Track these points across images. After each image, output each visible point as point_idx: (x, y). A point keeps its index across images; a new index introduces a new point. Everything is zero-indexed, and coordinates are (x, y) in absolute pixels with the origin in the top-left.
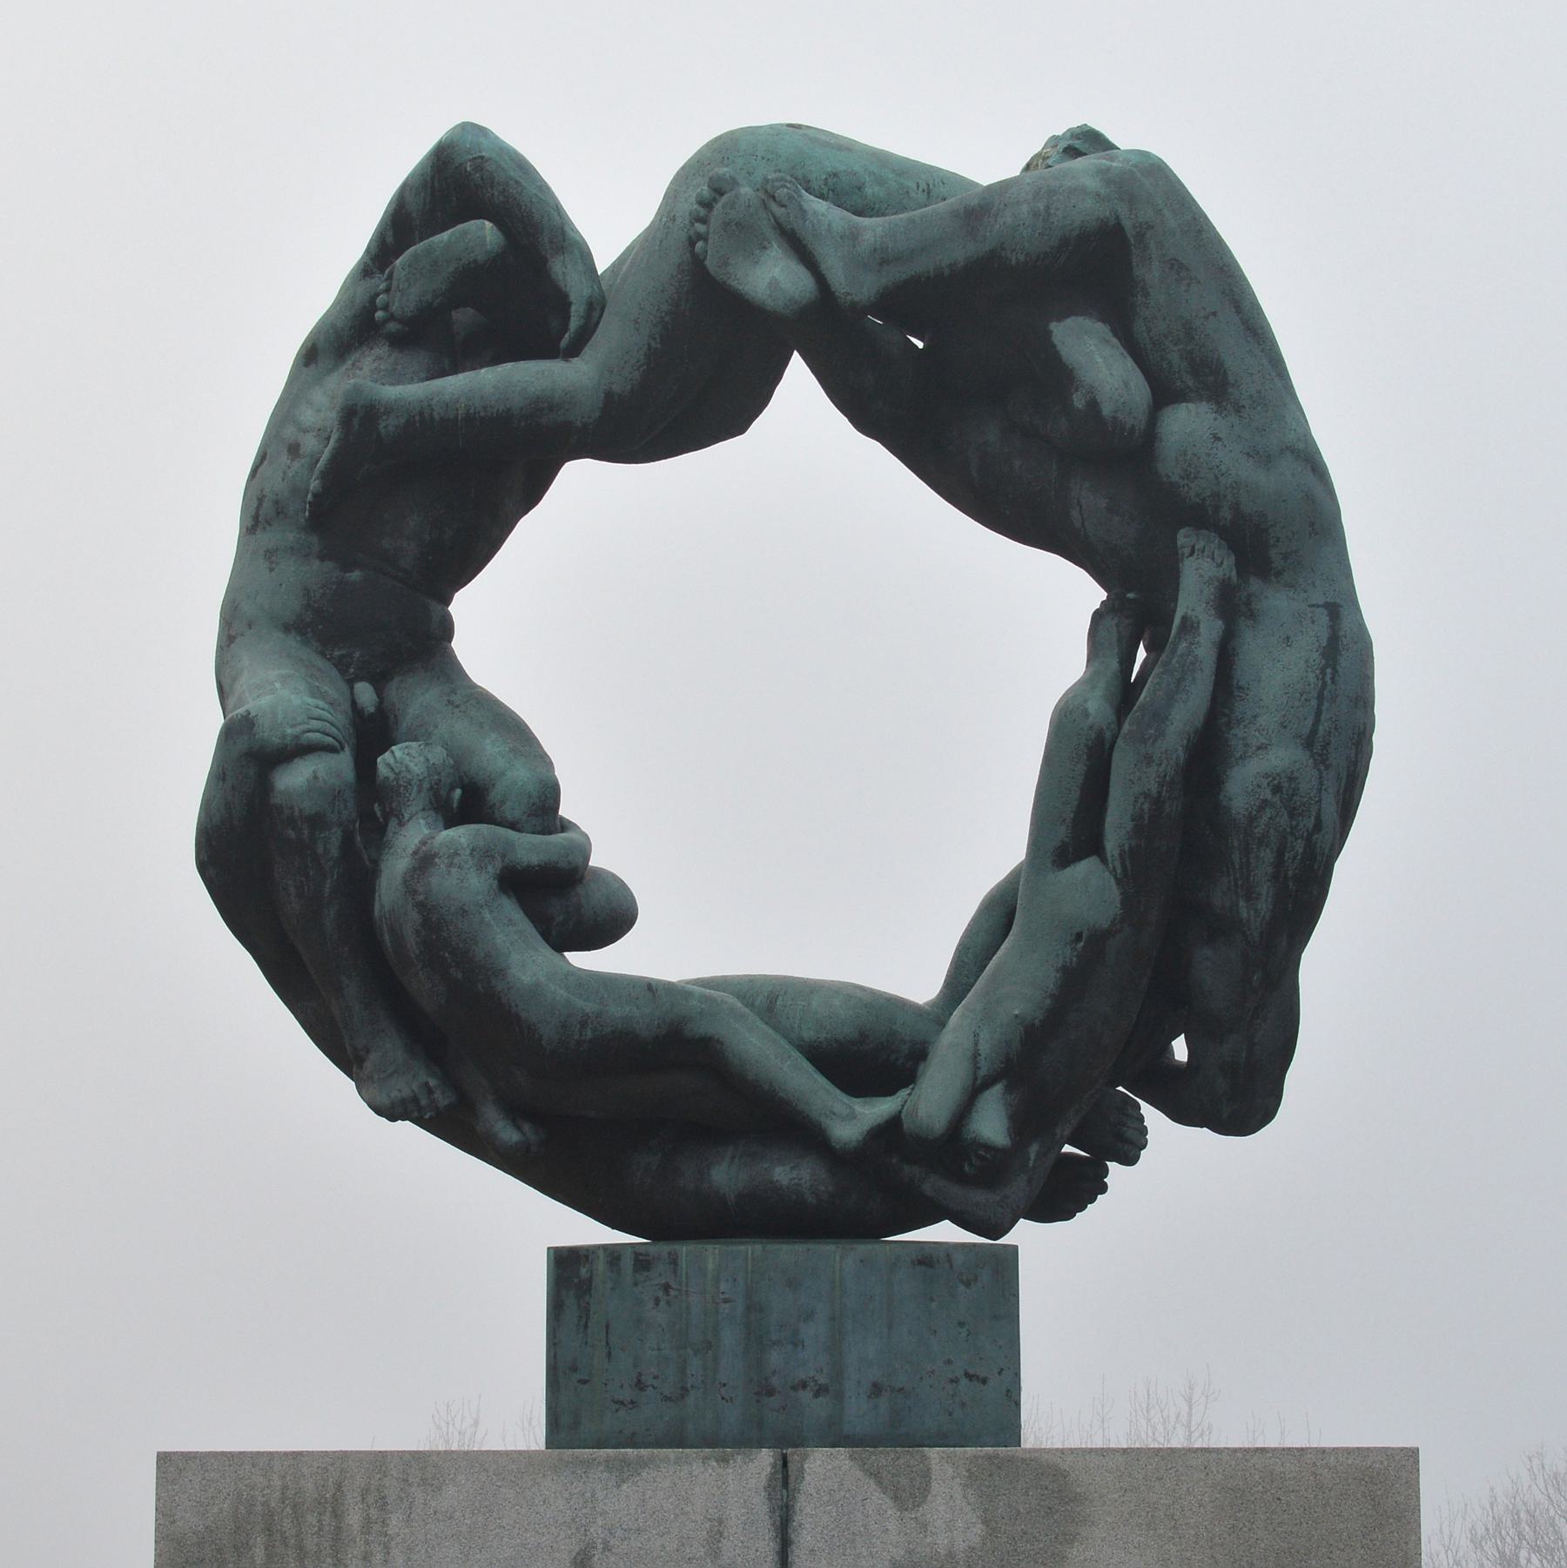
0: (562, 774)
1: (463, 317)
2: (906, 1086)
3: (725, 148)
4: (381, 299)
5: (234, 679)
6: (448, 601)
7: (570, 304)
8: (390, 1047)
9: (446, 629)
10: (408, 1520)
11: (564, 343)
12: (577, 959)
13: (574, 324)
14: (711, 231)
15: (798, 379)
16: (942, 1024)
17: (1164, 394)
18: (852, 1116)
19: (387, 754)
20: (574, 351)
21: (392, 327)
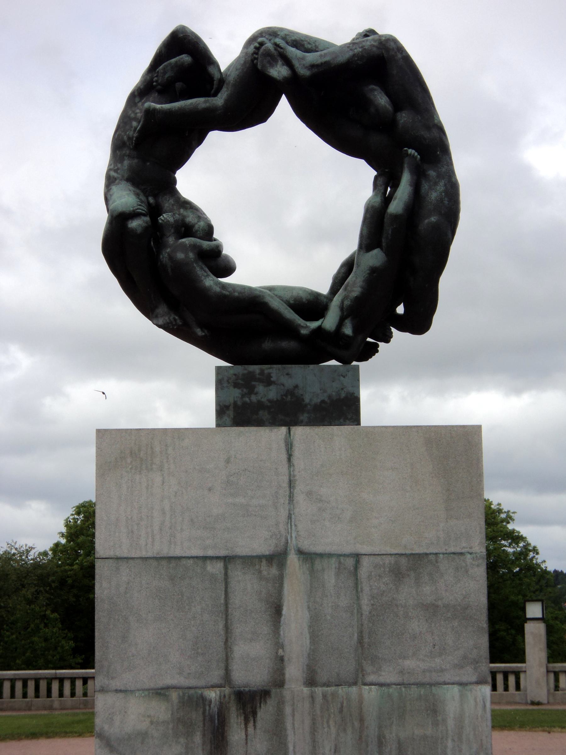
0: (213, 223)
1: (179, 85)
2: (322, 318)
3: (262, 33)
4: (155, 79)
5: (111, 195)
6: (175, 173)
8: (162, 309)
9: (174, 182)
10: (174, 449)
11: (213, 92)
12: (220, 279)
13: (215, 86)
14: (259, 57)
15: (284, 104)
16: (331, 300)
17: (397, 107)
19: (161, 216)
20: (215, 95)
21: (159, 87)
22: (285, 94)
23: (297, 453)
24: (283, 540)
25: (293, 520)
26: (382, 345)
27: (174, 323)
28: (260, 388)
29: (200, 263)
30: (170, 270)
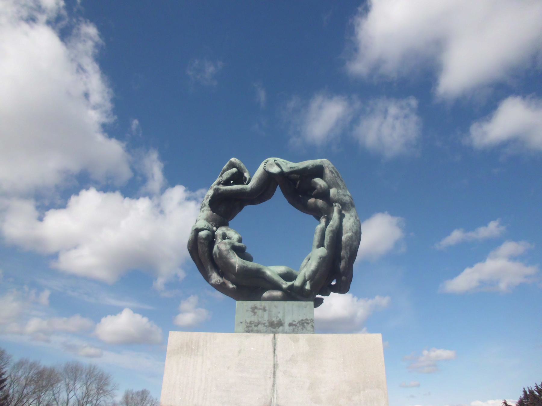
7: (246, 179)
13: (247, 181)
18: (286, 284)
20: (247, 184)
21: (222, 182)
22: (279, 186)
23: (278, 348)
24: (269, 399)
25: (275, 387)
26: (325, 298)
27: (219, 282)
28: (260, 312)
29: (233, 251)
30: (217, 254)
